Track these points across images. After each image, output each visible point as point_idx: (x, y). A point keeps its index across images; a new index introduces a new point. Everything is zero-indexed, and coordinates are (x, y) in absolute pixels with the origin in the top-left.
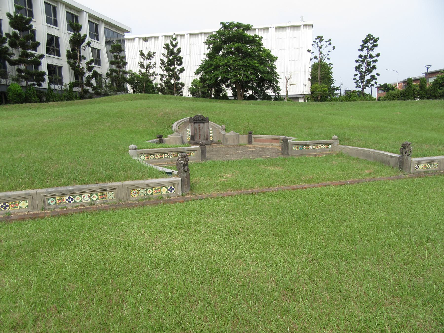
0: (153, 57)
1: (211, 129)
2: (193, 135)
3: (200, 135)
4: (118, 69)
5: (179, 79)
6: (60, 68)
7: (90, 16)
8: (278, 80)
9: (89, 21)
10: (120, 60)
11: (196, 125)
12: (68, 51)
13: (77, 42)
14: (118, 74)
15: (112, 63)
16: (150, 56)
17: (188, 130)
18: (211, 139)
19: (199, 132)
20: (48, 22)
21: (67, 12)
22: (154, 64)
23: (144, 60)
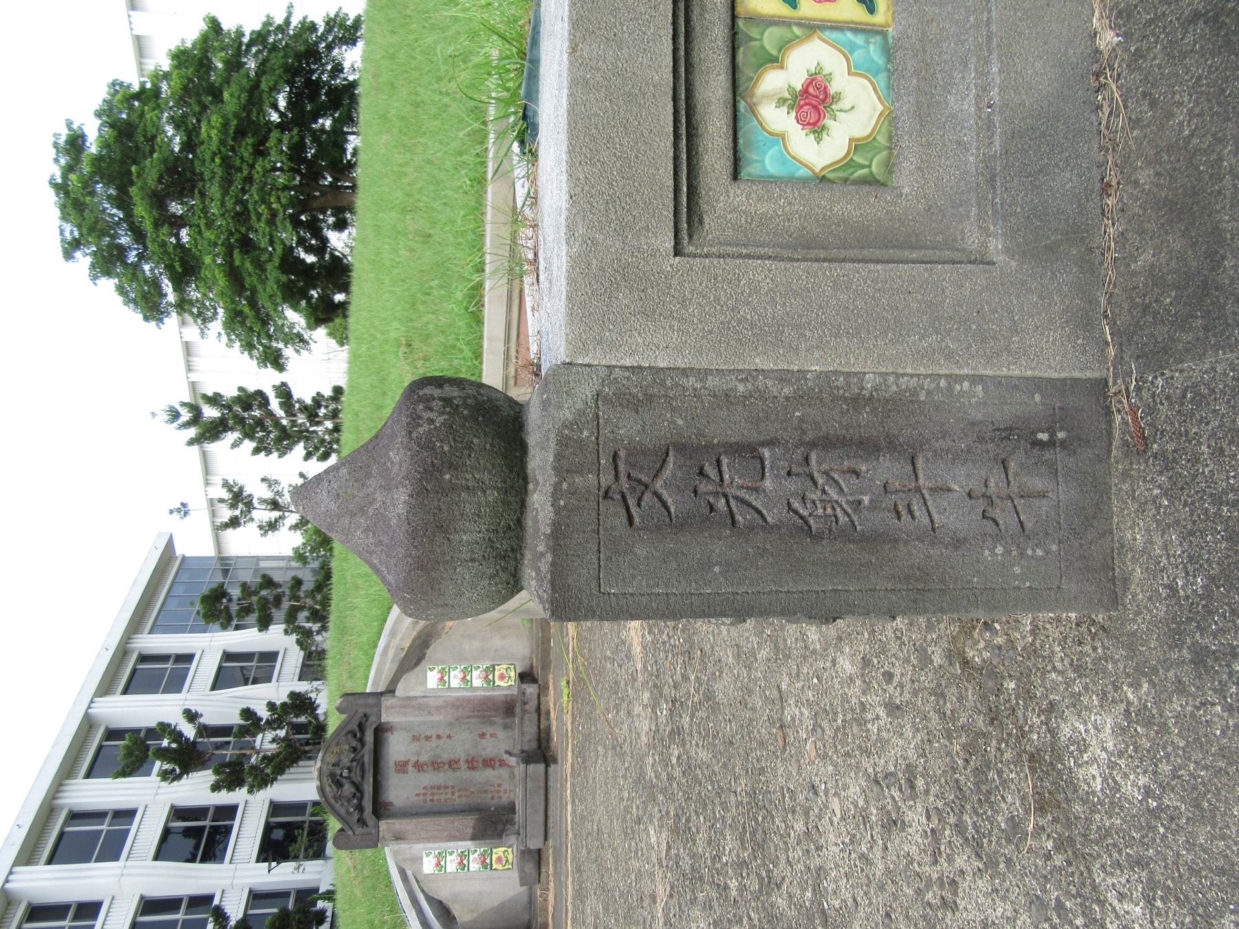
0: (241, 489)
2: (468, 823)
3: (472, 764)
4: (286, 604)
5: (318, 401)
6: (276, 808)
7: (105, 688)
8: (295, 21)
9: (125, 692)
10: (254, 599)
11: (399, 790)
12: (216, 788)
13: (186, 758)
14: (302, 608)
15: (264, 623)
16: (238, 497)
17: (428, 866)
18: (506, 682)
19: (453, 764)
20: (116, 857)
21: (88, 775)
22: (265, 485)
23: (252, 520)
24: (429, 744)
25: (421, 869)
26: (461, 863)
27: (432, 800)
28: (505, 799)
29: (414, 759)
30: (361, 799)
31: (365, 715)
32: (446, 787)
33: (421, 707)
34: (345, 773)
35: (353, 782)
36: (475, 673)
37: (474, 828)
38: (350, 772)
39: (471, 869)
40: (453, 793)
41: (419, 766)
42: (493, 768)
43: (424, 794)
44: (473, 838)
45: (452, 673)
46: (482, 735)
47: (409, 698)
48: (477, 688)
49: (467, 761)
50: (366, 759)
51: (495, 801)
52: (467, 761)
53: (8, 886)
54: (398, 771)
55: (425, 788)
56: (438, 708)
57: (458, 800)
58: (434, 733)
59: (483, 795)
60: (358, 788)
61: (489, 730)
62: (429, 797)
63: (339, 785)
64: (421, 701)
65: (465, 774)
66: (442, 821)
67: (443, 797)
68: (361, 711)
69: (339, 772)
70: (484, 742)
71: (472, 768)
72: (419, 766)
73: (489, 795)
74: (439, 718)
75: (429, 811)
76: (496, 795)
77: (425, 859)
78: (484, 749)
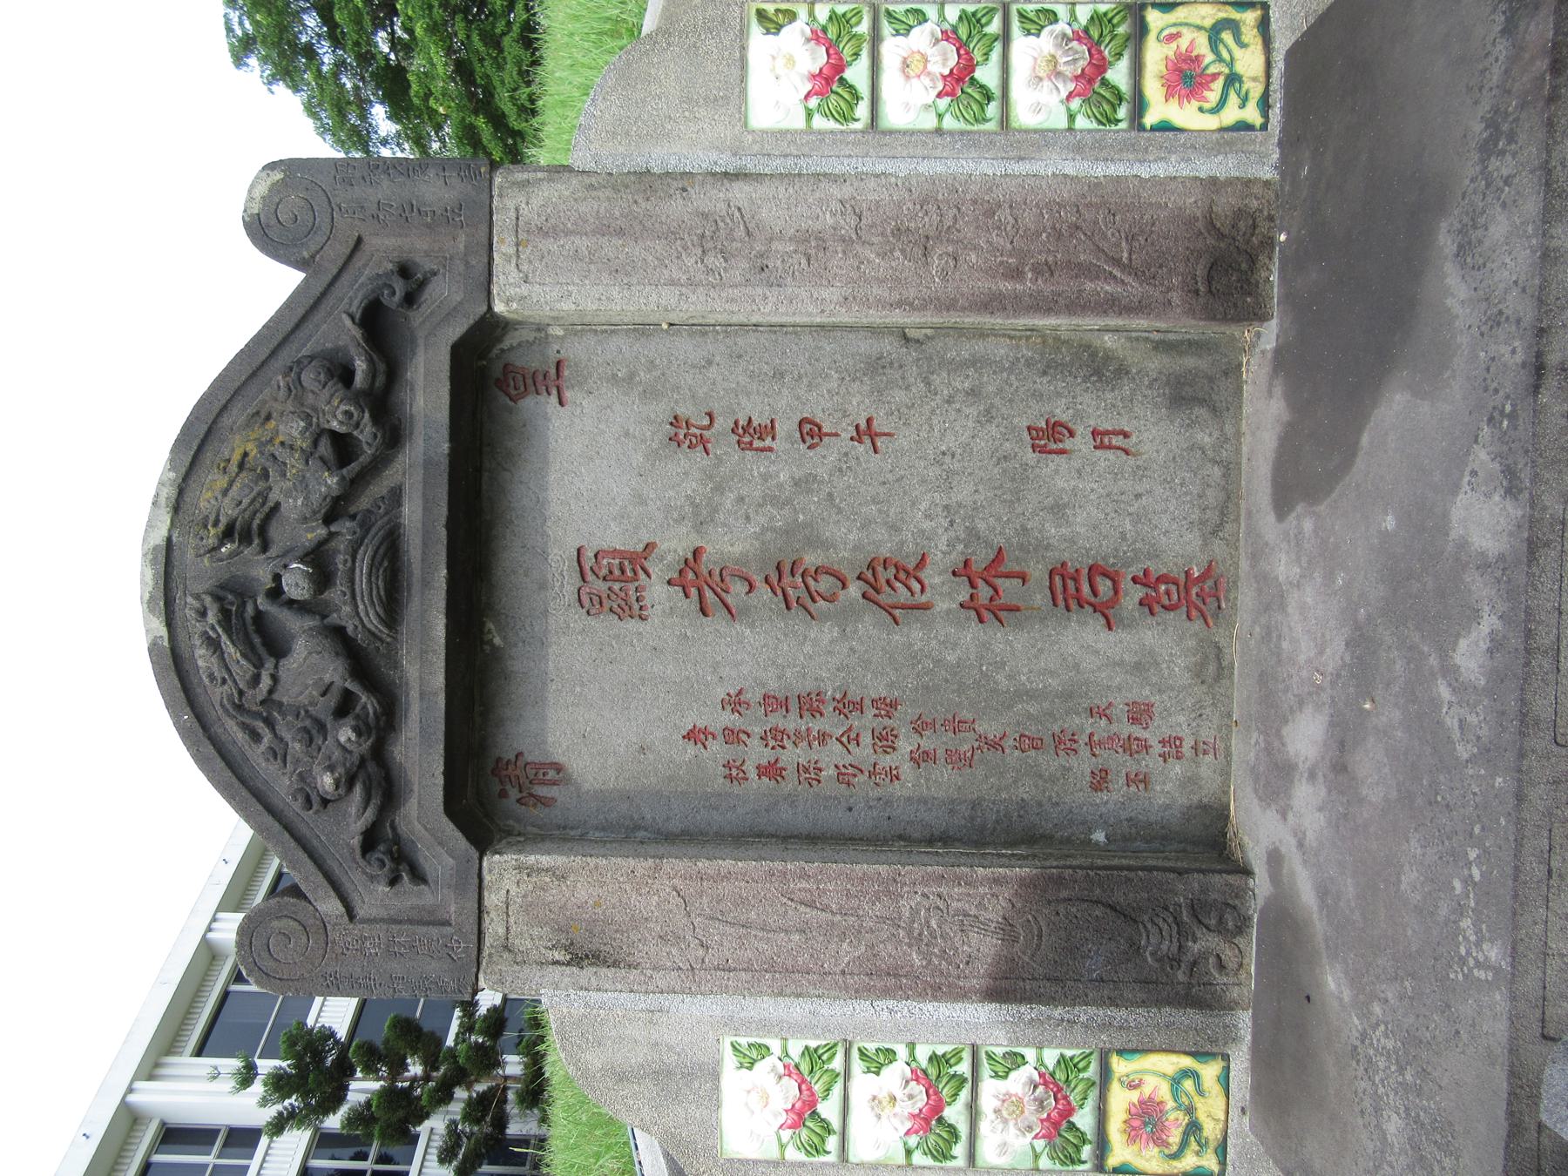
1: (777, 78)
2: (976, 903)
3: (989, 587)
11: (606, 700)
19: (887, 583)
24: (755, 465)
25: (712, 1129)
26: (931, 1117)
27: (771, 771)
28: (1169, 789)
29: (675, 544)
30: (384, 726)
31: (404, 271)
32: (847, 705)
33: (714, 239)
34: (296, 583)
35: (338, 633)
36: (1028, 51)
37: (1007, 930)
38: (322, 577)
39: (988, 1153)
40: (885, 741)
41: (700, 582)
42: (1107, 613)
43: (733, 736)
44: (1004, 988)
45: (893, 49)
46: (1050, 436)
47: (647, 181)
48: (1042, 139)
49: (963, 570)
50: (411, 513)
51: (1117, 793)
52: (963, 570)
53: (210, 935)
54: (592, 604)
55: (735, 703)
56: (814, 245)
57: (919, 783)
58: (781, 407)
59: (1049, 762)
60: (366, 666)
61: (1090, 408)
62: (756, 753)
63: (265, 643)
64: (714, 199)
65: (949, 637)
66: (834, 879)
67: (831, 756)
68: (384, 248)
69: (262, 574)
70: (1057, 474)
71: (988, 606)
72: (700, 582)
73: (1083, 764)
74: (809, 302)
75: (754, 819)
76: (1120, 763)
77: (733, 1080)
78: (1058, 510)
